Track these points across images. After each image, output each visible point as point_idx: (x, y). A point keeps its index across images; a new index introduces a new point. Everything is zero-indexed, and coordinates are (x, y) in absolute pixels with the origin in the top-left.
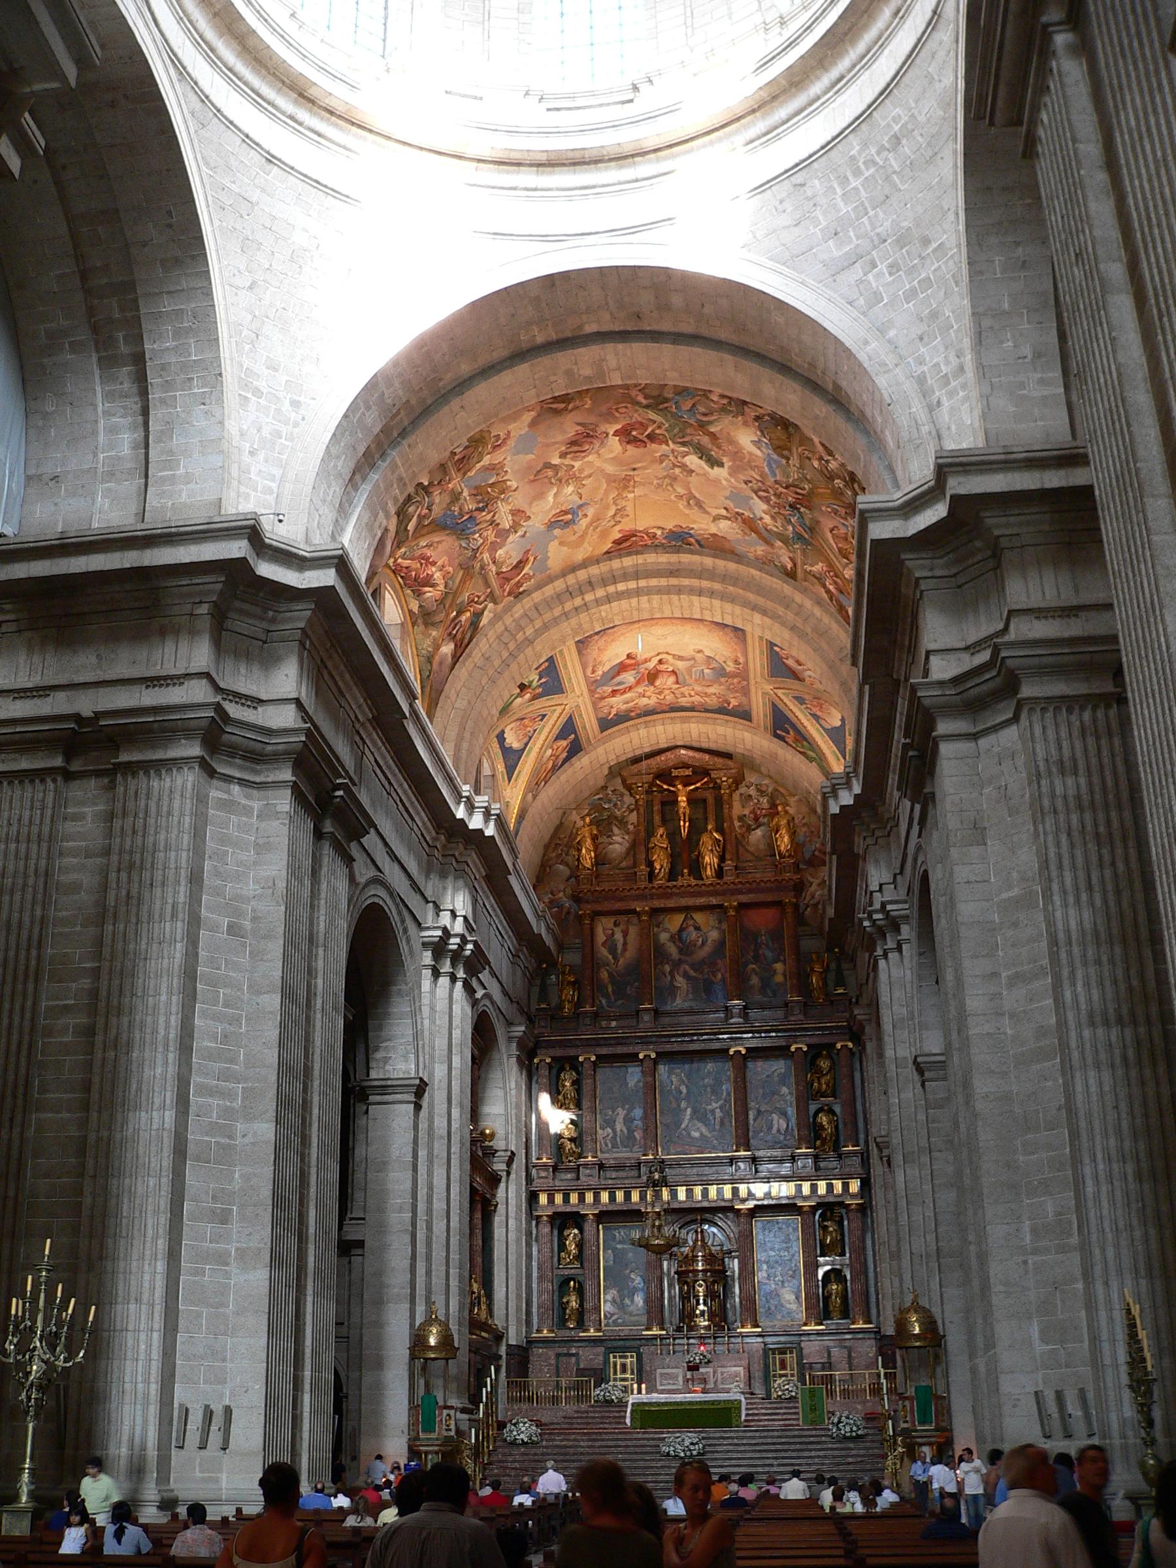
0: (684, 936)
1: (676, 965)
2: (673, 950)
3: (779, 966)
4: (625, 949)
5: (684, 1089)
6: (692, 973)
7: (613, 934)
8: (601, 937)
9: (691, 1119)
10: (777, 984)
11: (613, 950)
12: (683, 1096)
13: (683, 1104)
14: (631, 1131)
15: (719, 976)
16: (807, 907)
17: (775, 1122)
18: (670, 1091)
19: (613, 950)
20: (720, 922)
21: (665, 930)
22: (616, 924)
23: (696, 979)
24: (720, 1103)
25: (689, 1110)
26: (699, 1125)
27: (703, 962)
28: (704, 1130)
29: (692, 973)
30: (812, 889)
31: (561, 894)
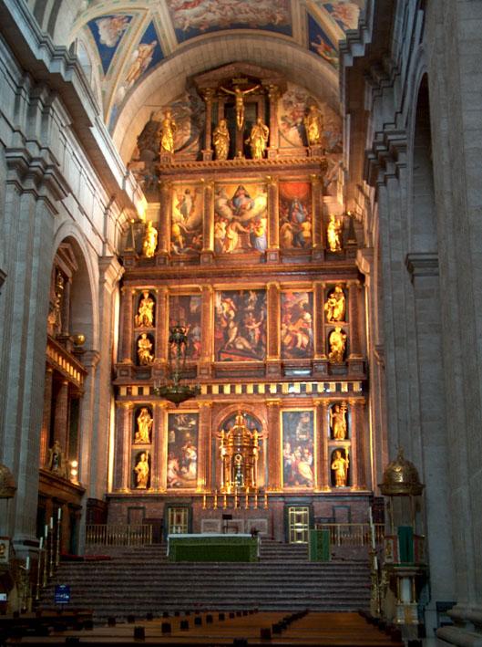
1: (230, 222)
2: (228, 212)
3: (306, 225)
4: (192, 211)
5: (232, 313)
6: (241, 229)
7: (184, 200)
9: (237, 336)
12: (232, 318)
13: (231, 325)
18: (222, 315)
19: (183, 211)
21: (223, 197)
22: (186, 193)
24: (259, 323)
25: (236, 329)
26: (243, 340)
27: (250, 221)
29: (241, 229)
30: (334, 169)
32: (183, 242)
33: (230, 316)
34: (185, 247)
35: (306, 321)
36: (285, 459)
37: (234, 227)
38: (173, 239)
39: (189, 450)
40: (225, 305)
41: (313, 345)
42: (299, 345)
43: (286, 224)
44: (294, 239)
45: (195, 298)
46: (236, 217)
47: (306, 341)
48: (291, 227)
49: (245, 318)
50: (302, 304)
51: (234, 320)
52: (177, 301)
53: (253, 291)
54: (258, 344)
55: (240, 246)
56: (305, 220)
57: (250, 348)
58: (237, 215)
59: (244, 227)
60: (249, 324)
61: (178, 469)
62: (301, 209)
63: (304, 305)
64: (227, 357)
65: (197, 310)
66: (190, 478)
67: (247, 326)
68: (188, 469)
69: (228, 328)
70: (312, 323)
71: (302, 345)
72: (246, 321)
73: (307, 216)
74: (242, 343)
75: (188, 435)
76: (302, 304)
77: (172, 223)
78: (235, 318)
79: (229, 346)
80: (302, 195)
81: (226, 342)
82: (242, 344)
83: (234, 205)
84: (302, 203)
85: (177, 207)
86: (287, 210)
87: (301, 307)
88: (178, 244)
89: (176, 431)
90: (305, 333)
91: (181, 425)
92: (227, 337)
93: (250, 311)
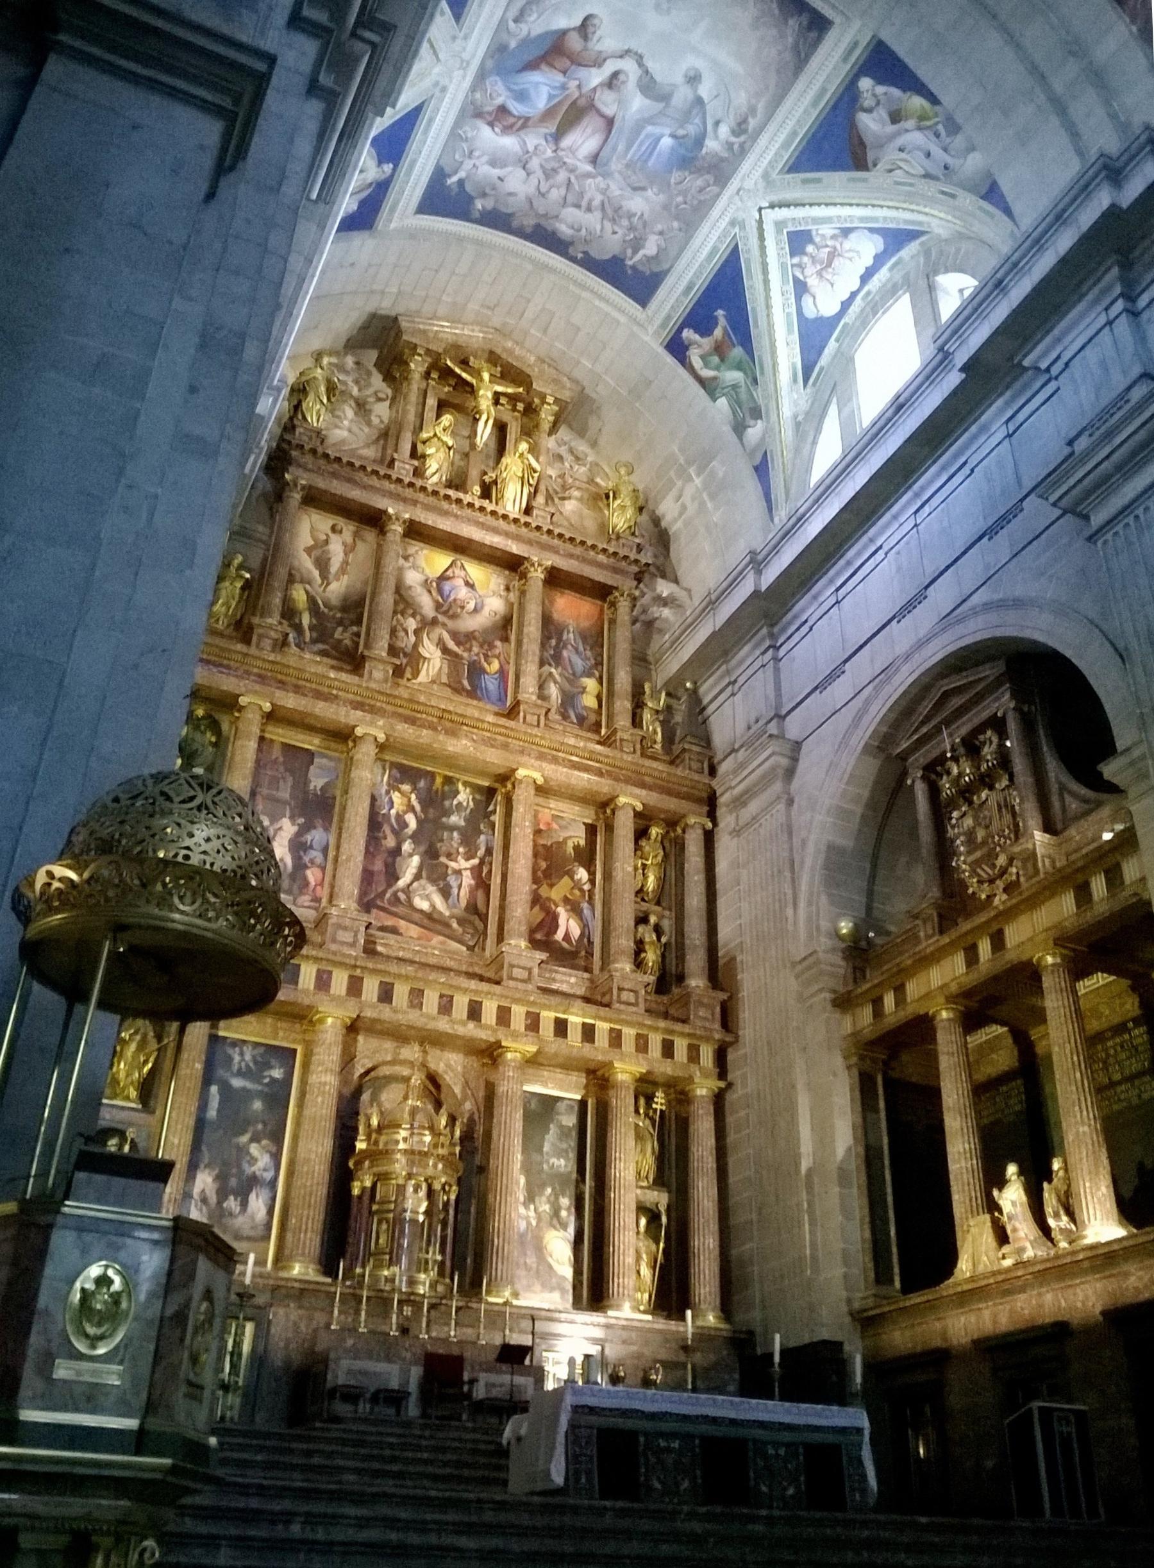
0: (447, 587)
4: (343, 570)
5: (412, 822)
6: (451, 645)
7: (327, 542)
9: (417, 877)
10: (585, 708)
11: (322, 564)
13: (407, 847)
15: (495, 665)
17: (562, 921)
18: (387, 816)
20: (508, 589)
21: (415, 567)
22: (334, 529)
23: (456, 655)
25: (416, 860)
26: (431, 889)
28: (438, 900)
29: (451, 645)
32: (312, 628)
33: (406, 825)
34: (314, 641)
35: (577, 885)
38: (289, 613)
39: (254, 1149)
40: (396, 797)
41: (590, 943)
42: (559, 935)
45: (324, 761)
46: (441, 618)
47: (576, 931)
49: (442, 840)
50: (570, 844)
51: (415, 837)
52: (276, 753)
54: (467, 909)
55: (444, 680)
56: (589, 675)
57: (447, 914)
58: (445, 613)
59: (458, 644)
61: (213, 1199)
63: (576, 848)
66: (247, 1232)
67: (443, 859)
68: (244, 1204)
69: (397, 851)
71: (567, 938)
72: (442, 847)
74: (428, 897)
75: (258, 1105)
76: (570, 844)
77: (291, 580)
79: (395, 894)
80: (585, 624)
81: (389, 886)
82: (427, 899)
83: (440, 591)
84: (584, 638)
85: (309, 551)
86: (553, 642)
87: (570, 850)
90: (575, 909)
91: (240, 1074)
92: (392, 875)
93: (452, 829)
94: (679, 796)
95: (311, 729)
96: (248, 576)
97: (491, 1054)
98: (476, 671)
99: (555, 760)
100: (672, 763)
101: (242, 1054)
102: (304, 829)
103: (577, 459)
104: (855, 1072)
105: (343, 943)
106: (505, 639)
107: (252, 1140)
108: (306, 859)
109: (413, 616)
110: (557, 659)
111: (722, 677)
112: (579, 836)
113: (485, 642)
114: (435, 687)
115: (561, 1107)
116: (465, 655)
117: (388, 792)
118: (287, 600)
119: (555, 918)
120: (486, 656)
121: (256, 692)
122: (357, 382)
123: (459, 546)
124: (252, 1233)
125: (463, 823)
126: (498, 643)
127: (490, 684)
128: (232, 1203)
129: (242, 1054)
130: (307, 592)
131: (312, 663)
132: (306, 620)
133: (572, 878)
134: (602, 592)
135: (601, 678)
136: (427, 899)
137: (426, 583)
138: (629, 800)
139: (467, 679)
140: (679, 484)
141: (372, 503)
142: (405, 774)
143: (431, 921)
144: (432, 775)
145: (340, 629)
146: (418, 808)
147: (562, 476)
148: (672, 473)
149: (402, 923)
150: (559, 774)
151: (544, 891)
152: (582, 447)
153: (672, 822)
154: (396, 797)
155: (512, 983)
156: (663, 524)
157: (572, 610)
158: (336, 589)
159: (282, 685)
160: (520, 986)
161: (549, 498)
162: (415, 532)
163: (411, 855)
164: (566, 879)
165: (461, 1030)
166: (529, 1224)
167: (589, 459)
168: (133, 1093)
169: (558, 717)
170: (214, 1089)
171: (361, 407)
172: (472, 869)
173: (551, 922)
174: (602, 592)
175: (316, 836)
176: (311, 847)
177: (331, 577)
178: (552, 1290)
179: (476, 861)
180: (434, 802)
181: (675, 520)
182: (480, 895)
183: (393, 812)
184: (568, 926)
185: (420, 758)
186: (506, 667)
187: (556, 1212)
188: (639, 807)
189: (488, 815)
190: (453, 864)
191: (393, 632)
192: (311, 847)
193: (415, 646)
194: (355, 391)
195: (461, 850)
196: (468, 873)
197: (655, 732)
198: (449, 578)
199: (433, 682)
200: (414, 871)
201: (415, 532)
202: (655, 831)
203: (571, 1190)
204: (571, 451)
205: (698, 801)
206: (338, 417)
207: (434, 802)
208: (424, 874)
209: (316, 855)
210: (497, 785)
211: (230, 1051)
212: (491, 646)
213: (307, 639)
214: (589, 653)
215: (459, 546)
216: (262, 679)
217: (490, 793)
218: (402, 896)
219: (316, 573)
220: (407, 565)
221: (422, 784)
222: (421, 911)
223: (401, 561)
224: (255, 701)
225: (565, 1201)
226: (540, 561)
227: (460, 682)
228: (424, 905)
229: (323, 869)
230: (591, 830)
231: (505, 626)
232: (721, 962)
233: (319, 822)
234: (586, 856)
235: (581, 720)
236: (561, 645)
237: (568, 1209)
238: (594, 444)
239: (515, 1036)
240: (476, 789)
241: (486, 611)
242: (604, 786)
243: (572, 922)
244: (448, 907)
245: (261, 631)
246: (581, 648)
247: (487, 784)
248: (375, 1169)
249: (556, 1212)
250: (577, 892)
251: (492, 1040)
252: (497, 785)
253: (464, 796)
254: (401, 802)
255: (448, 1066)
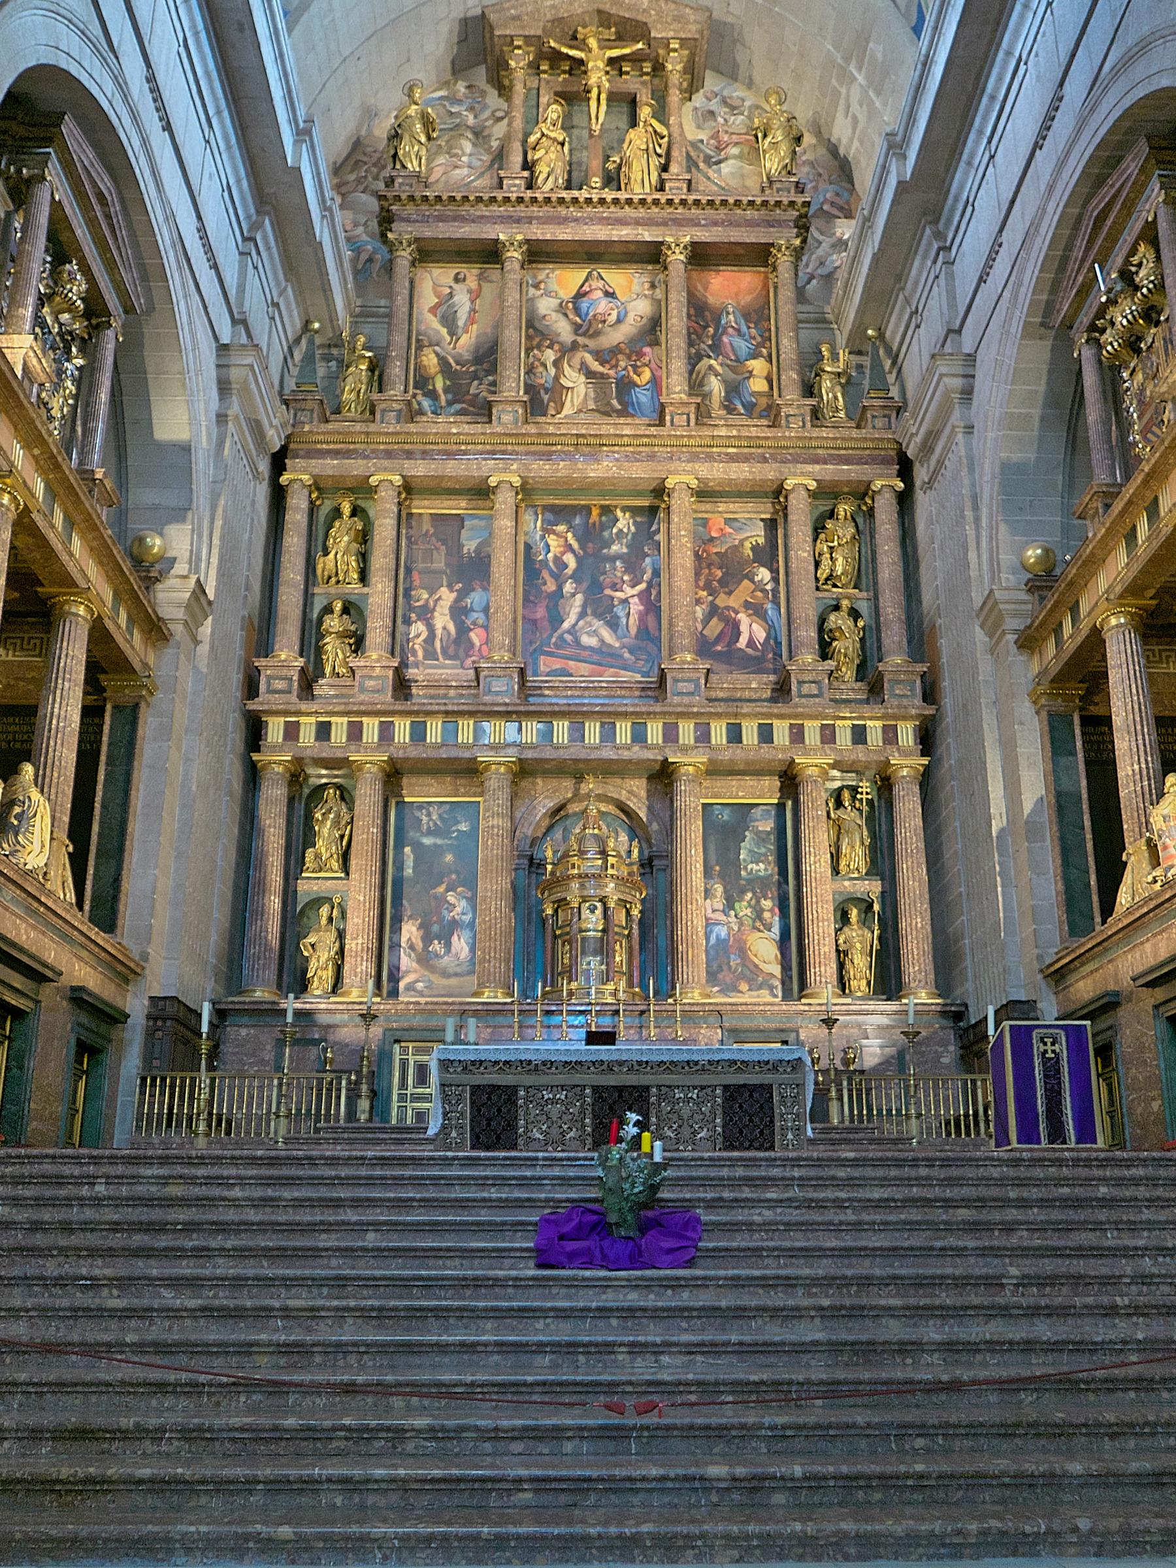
2: (563, 329)
3: (758, 366)
4: (471, 320)
5: (570, 560)
6: (596, 366)
7: (451, 295)
8: (427, 298)
9: (583, 615)
10: (754, 394)
11: (449, 321)
12: (569, 571)
13: (569, 587)
14: (463, 630)
15: (647, 375)
16: (812, 277)
17: (744, 628)
19: (449, 321)
20: (653, 286)
21: (547, 294)
23: (602, 376)
25: (579, 598)
26: (597, 624)
27: (615, 351)
28: (607, 635)
29: (596, 366)
31: (361, 229)
32: (446, 390)
34: (450, 403)
36: (709, 924)
37: (576, 361)
38: (423, 382)
39: (451, 898)
40: (552, 540)
41: (778, 644)
42: (742, 642)
43: (705, 362)
44: (728, 397)
45: (476, 522)
46: (580, 340)
47: (760, 634)
48: (718, 368)
50: (748, 545)
51: (575, 576)
53: (625, 509)
54: (637, 637)
56: (755, 356)
60: (615, 587)
61: (419, 945)
62: (744, 329)
64: (557, 664)
65: (478, 550)
67: (608, 592)
68: (448, 945)
70: (775, 591)
71: (751, 643)
73: (758, 346)
74: (595, 633)
75: (449, 858)
76: (748, 545)
78: (575, 571)
79: (561, 638)
80: (746, 299)
83: (577, 311)
84: (747, 316)
87: (748, 552)
88: (433, 395)
89: (418, 847)
90: (757, 611)
91: (429, 833)
92: (556, 620)
93: (613, 559)
94: (860, 461)
95: (451, 492)
96: (370, 354)
97: (663, 776)
98: (625, 386)
99: (710, 458)
100: (858, 427)
101: (429, 815)
102: (462, 595)
103: (733, 108)
104: (1044, 714)
105: (498, 693)
106: (656, 343)
107: (447, 890)
108: (468, 622)
109: (550, 347)
110: (717, 348)
111: (902, 310)
112: (757, 534)
113: (632, 352)
114: (582, 415)
115: (757, 813)
116: (612, 372)
117: (543, 537)
118: (419, 367)
119: (736, 625)
120: (635, 367)
121: (385, 470)
122: (471, 109)
123: (592, 254)
124: (458, 970)
125: (625, 550)
126: (647, 350)
127: (642, 397)
128: (436, 946)
129: (429, 815)
130: (437, 354)
131: (450, 425)
132: (439, 383)
133: (753, 582)
134: (760, 255)
135: (770, 355)
136: (594, 635)
137: (561, 309)
138: (800, 480)
139: (617, 397)
140: (843, 91)
141: (485, 236)
142: (559, 513)
143: (604, 656)
144: (588, 509)
145: (476, 382)
146: (576, 545)
147: (715, 136)
148: (834, 82)
149: (571, 663)
150: (715, 472)
151: (722, 601)
152: (737, 92)
153: (862, 492)
154: (552, 540)
155: (676, 699)
156: (842, 151)
157: (728, 288)
158: (466, 342)
159: (409, 455)
160: (686, 700)
161: (691, 163)
162: (539, 254)
163: (573, 595)
164: (746, 582)
165: (626, 755)
166: (730, 929)
167: (747, 104)
168: (335, 866)
169: (723, 412)
170: (407, 850)
171: (479, 134)
172: (639, 595)
173: (734, 629)
174: (760, 255)
175: (476, 598)
176: (472, 610)
177: (460, 331)
178: (760, 987)
179: (643, 586)
180: (592, 537)
181: (851, 140)
182: (651, 621)
183: (550, 555)
184: (752, 630)
185: (569, 493)
186: (657, 374)
187: (759, 913)
188: (813, 485)
189: (651, 535)
190: (619, 594)
191: (530, 371)
192: (472, 610)
193: (556, 378)
194: (471, 120)
195: (626, 578)
196: (636, 599)
197: (836, 398)
198: (586, 294)
199: (580, 411)
200: (578, 610)
201: (539, 254)
202: (843, 509)
203: (773, 892)
204: (724, 102)
205: (885, 461)
206: (456, 155)
207: (592, 537)
208: (589, 611)
209: (479, 617)
210: (656, 502)
211: (418, 814)
212: (640, 355)
213: (443, 403)
214: (753, 331)
215: (592, 254)
216: (389, 455)
217: (653, 511)
218: (568, 637)
219: (444, 331)
220: (539, 293)
221: (578, 520)
222: (591, 649)
223: (532, 291)
224: (386, 478)
225: (767, 904)
226: (677, 242)
227: (609, 404)
228: (588, 640)
229: (486, 628)
230: (771, 525)
231: (653, 329)
232: (927, 632)
233: (476, 584)
234: (768, 554)
235: (750, 408)
236: (720, 331)
237: (771, 910)
238: (750, 85)
239: (685, 750)
240: (634, 511)
241: (630, 319)
242: (769, 472)
243: (754, 626)
244: (618, 638)
245: (383, 406)
246: (744, 329)
247: (646, 503)
248: (554, 897)
249: (759, 913)
250: (759, 594)
251: (660, 758)
252: (656, 502)
253: (624, 522)
254: (558, 545)
255: (630, 792)
